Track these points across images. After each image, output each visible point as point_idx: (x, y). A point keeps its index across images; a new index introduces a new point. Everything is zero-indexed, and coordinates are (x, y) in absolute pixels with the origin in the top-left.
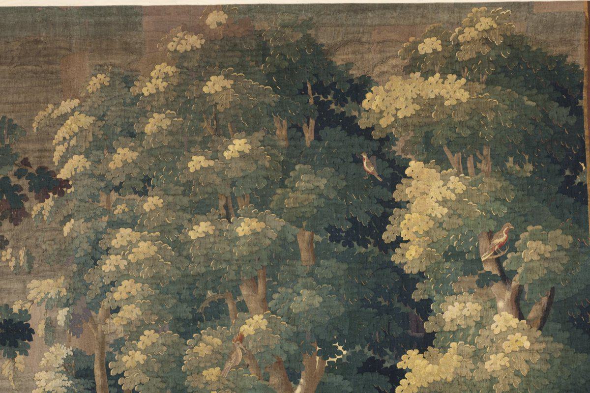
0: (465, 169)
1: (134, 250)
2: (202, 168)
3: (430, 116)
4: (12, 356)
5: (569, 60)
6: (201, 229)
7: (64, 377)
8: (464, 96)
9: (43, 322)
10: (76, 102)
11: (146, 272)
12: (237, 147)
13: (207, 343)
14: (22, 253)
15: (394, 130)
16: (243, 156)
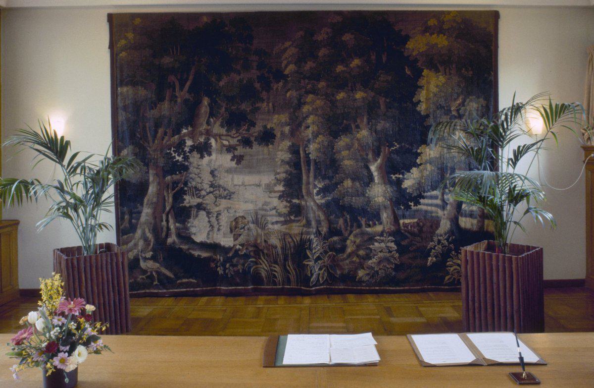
0: (445, 73)
1: (315, 103)
2: (342, 71)
3: (432, 51)
4: (267, 145)
5: (487, 30)
6: (341, 96)
7: (289, 154)
8: (446, 43)
9: (280, 132)
10: (291, 43)
11: (320, 112)
12: (356, 63)
13: (343, 141)
14: (271, 104)
15: (418, 57)
16: (358, 66)
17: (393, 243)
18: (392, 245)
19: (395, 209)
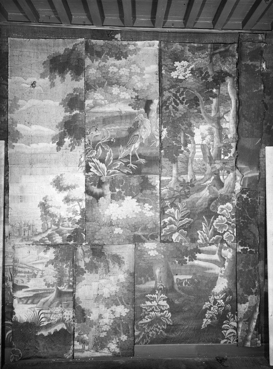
17: (166, 302)
18: (165, 303)
19: (170, 263)
